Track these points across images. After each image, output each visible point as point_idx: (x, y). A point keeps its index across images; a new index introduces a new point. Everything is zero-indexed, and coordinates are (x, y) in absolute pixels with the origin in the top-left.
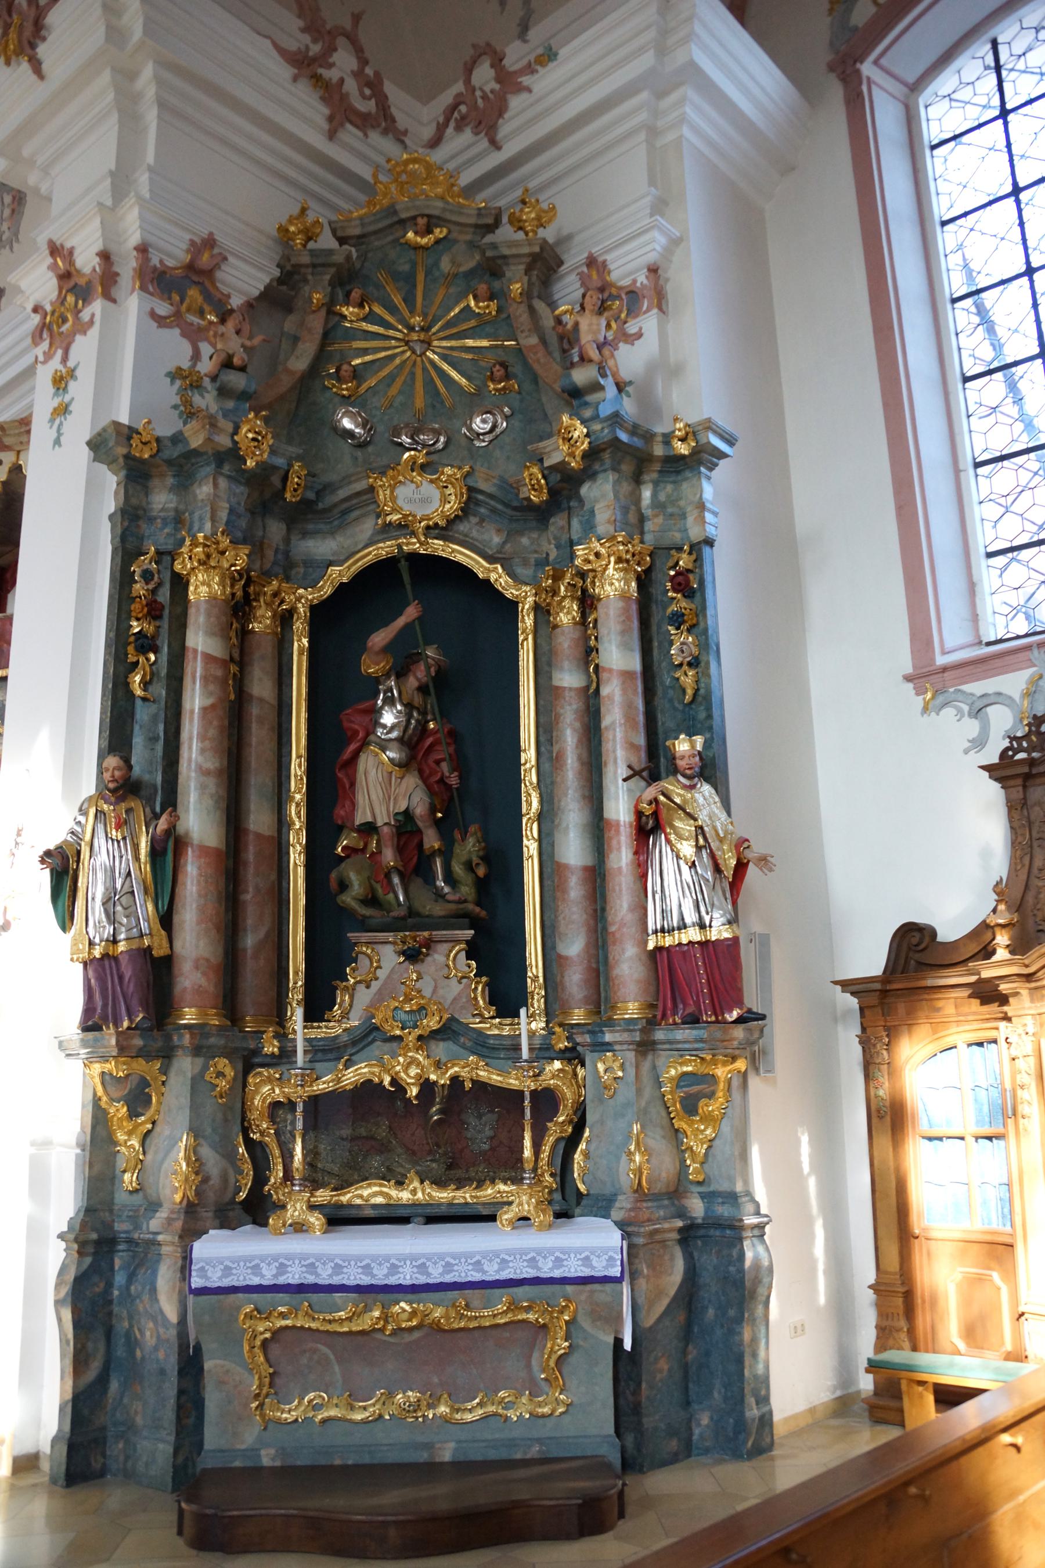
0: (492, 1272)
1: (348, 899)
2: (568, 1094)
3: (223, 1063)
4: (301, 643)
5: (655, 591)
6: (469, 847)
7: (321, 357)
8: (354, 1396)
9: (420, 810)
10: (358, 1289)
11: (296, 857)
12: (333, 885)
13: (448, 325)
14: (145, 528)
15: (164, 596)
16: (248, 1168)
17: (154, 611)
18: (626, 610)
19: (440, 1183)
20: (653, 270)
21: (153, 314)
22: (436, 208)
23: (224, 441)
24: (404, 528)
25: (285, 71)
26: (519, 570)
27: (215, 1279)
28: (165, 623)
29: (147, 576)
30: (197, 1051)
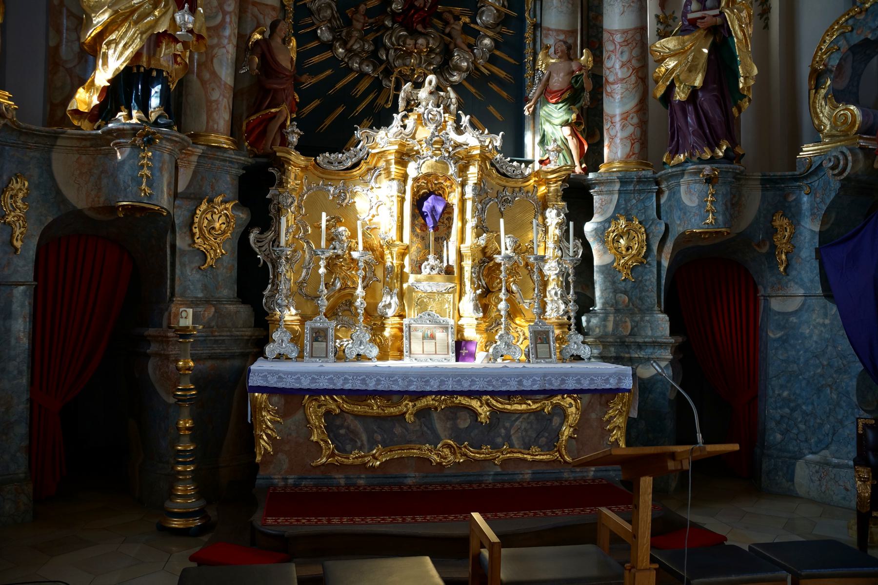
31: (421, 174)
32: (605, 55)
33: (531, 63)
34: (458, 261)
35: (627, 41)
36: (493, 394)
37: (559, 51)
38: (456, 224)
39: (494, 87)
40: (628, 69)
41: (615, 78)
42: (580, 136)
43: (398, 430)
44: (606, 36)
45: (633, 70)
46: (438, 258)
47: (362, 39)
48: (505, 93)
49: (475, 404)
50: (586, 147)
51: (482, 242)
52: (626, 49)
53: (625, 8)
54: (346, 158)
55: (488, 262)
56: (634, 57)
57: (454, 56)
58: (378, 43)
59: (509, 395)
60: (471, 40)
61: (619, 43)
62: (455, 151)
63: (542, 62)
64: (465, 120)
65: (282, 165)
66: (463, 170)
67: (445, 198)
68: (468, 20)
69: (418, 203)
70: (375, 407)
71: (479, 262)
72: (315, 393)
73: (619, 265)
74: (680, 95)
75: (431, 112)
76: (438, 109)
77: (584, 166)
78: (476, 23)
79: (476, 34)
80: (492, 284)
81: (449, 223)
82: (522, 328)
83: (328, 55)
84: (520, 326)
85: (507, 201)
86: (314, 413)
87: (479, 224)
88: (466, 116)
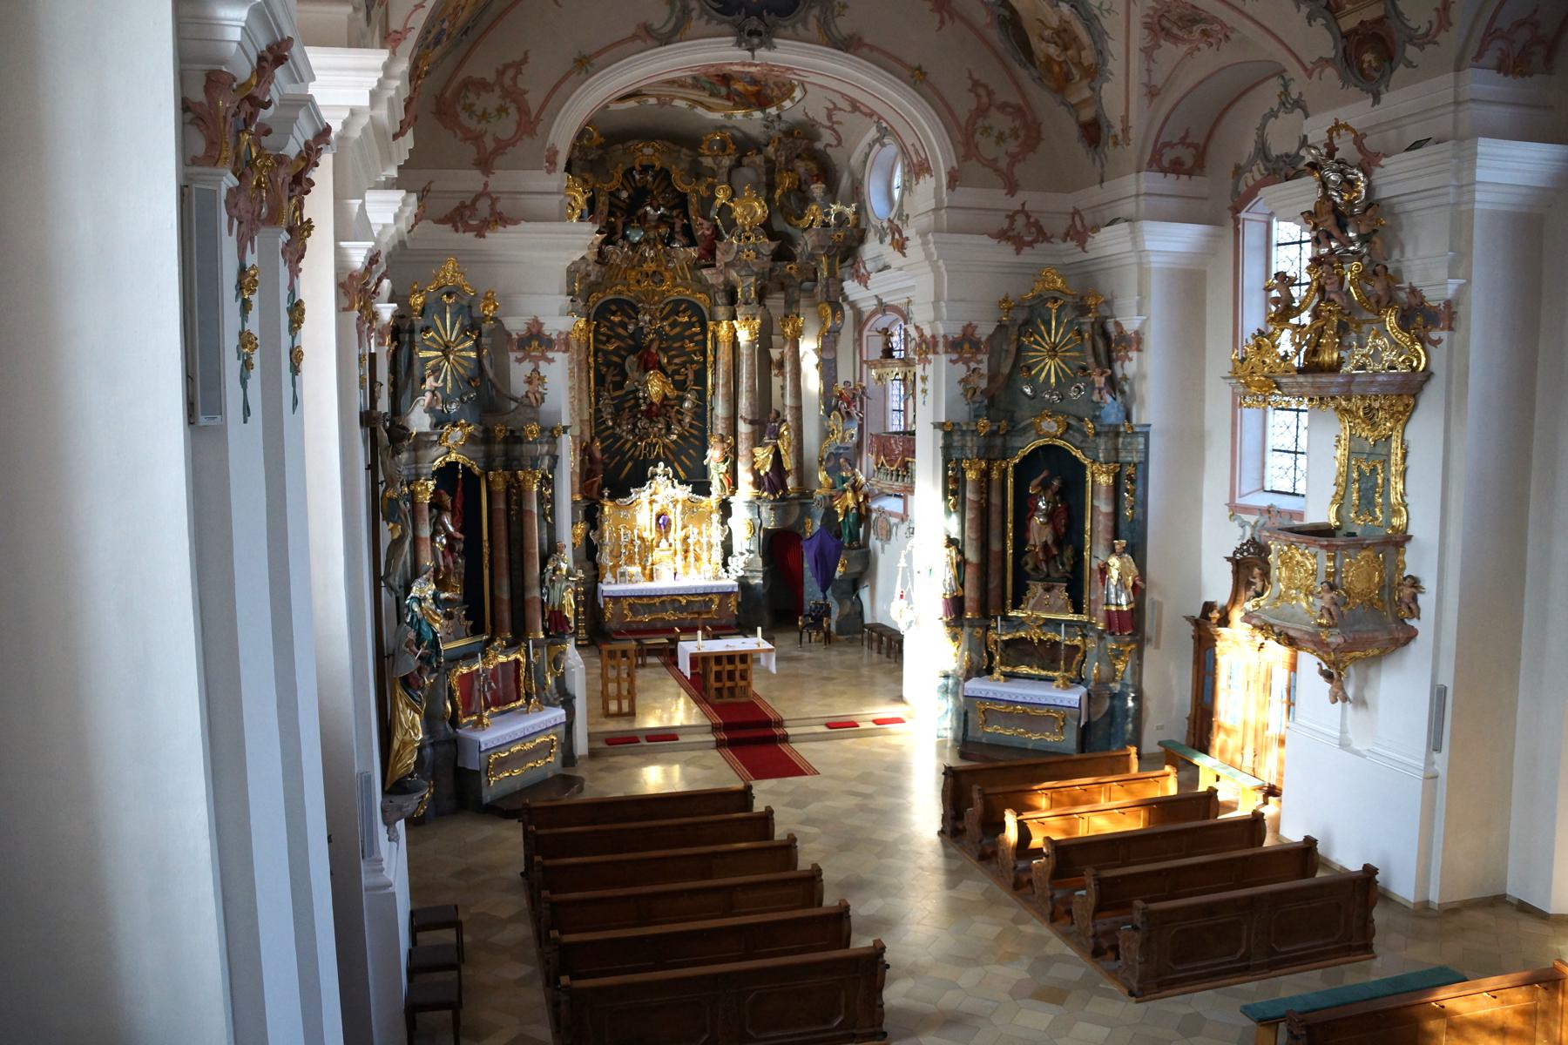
0: (1043, 701)
1: (1028, 568)
2: (1082, 646)
3: (978, 629)
4: (1010, 481)
5: (1122, 480)
6: (1069, 552)
7: (1015, 365)
8: (1007, 728)
9: (1050, 542)
10: (1007, 701)
11: (1010, 559)
12: (1022, 563)
13: (1065, 345)
14: (952, 451)
15: (959, 475)
16: (986, 660)
17: (956, 481)
18: (1107, 491)
19: (1044, 669)
20: (1137, 333)
21: (951, 361)
22: (1057, 295)
23: (973, 428)
24: (1047, 435)
25: (995, 241)
26: (1087, 453)
27: (970, 694)
28: (960, 485)
29: (953, 470)
30: (970, 626)
36: (687, 595)
38: (673, 527)
39: (692, 440)
43: (654, 608)
47: (628, 424)
49: (680, 598)
54: (627, 501)
58: (635, 425)
59: (692, 595)
60: (680, 417)
64: (676, 482)
65: (603, 506)
66: (675, 505)
69: (658, 519)
70: (645, 601)
72: (625, 597)
74: (762, 473)
79: (682, 414)
83: (610, 431)
86: (625, 604)
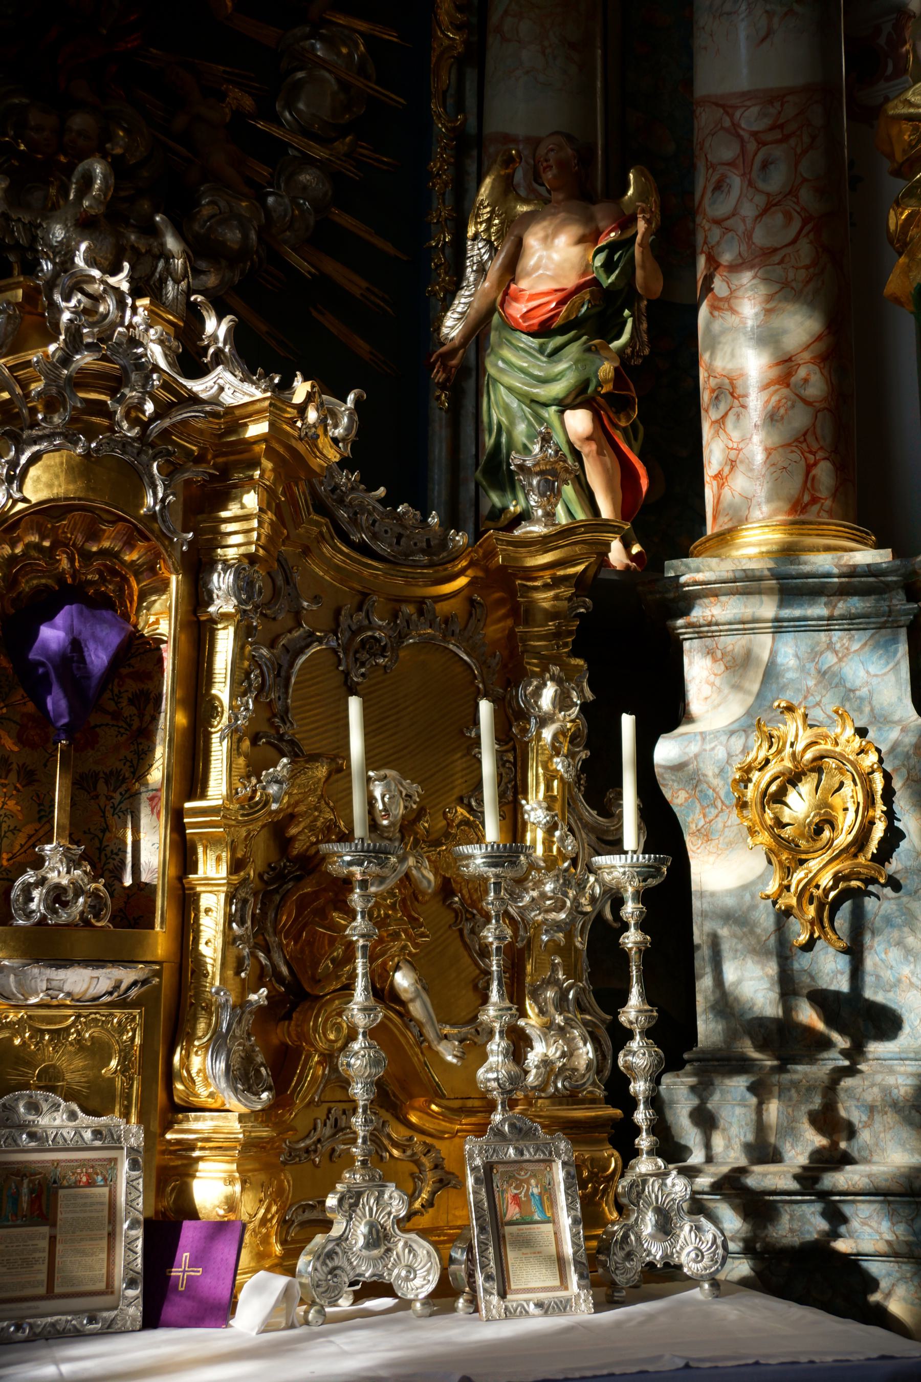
31: (20, 506)
32: (702, 180)
33: (448, 251)
34: (172, 872)
35: (781, 127)
37: (552, 162)
40: (788, 217)
41: (744, 248)
42: (624, 447)
44: (705, 118)
45: (805, 222)
46: (84, 857)
48: (361, 342)
50: (644, 483)
51: (273, 789)
52: (778, 152)
53: (776, 20)
55: (299, 879)
56: (805, 180)
57: (197, 204)
61: (754, 134)
62: (167, 423)
63: (492, 212)
67: (126, 617)
68: (248, 103)
71: (260, 876)
73: (788, 888)
75: (85, 287)
76: (112, 281)
77: (636, 549)
78: (276, 120)
80: (316, 964)
81: (141, 716)
82: (429, 1140)
84: (423, 1132)
85: (373, 647)
87: (265, 728)
88: (220, 319)
